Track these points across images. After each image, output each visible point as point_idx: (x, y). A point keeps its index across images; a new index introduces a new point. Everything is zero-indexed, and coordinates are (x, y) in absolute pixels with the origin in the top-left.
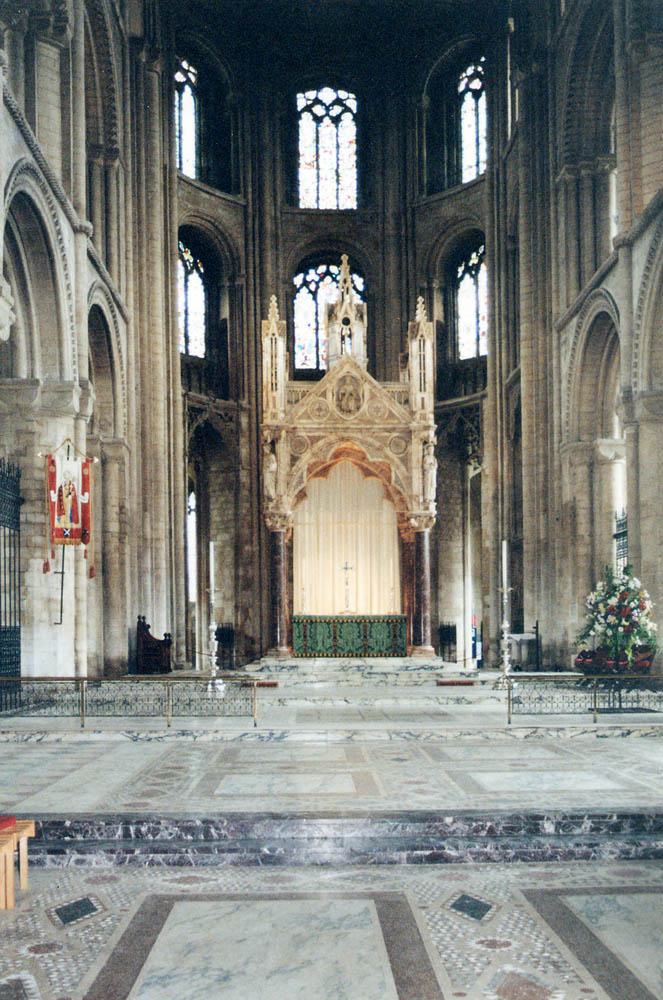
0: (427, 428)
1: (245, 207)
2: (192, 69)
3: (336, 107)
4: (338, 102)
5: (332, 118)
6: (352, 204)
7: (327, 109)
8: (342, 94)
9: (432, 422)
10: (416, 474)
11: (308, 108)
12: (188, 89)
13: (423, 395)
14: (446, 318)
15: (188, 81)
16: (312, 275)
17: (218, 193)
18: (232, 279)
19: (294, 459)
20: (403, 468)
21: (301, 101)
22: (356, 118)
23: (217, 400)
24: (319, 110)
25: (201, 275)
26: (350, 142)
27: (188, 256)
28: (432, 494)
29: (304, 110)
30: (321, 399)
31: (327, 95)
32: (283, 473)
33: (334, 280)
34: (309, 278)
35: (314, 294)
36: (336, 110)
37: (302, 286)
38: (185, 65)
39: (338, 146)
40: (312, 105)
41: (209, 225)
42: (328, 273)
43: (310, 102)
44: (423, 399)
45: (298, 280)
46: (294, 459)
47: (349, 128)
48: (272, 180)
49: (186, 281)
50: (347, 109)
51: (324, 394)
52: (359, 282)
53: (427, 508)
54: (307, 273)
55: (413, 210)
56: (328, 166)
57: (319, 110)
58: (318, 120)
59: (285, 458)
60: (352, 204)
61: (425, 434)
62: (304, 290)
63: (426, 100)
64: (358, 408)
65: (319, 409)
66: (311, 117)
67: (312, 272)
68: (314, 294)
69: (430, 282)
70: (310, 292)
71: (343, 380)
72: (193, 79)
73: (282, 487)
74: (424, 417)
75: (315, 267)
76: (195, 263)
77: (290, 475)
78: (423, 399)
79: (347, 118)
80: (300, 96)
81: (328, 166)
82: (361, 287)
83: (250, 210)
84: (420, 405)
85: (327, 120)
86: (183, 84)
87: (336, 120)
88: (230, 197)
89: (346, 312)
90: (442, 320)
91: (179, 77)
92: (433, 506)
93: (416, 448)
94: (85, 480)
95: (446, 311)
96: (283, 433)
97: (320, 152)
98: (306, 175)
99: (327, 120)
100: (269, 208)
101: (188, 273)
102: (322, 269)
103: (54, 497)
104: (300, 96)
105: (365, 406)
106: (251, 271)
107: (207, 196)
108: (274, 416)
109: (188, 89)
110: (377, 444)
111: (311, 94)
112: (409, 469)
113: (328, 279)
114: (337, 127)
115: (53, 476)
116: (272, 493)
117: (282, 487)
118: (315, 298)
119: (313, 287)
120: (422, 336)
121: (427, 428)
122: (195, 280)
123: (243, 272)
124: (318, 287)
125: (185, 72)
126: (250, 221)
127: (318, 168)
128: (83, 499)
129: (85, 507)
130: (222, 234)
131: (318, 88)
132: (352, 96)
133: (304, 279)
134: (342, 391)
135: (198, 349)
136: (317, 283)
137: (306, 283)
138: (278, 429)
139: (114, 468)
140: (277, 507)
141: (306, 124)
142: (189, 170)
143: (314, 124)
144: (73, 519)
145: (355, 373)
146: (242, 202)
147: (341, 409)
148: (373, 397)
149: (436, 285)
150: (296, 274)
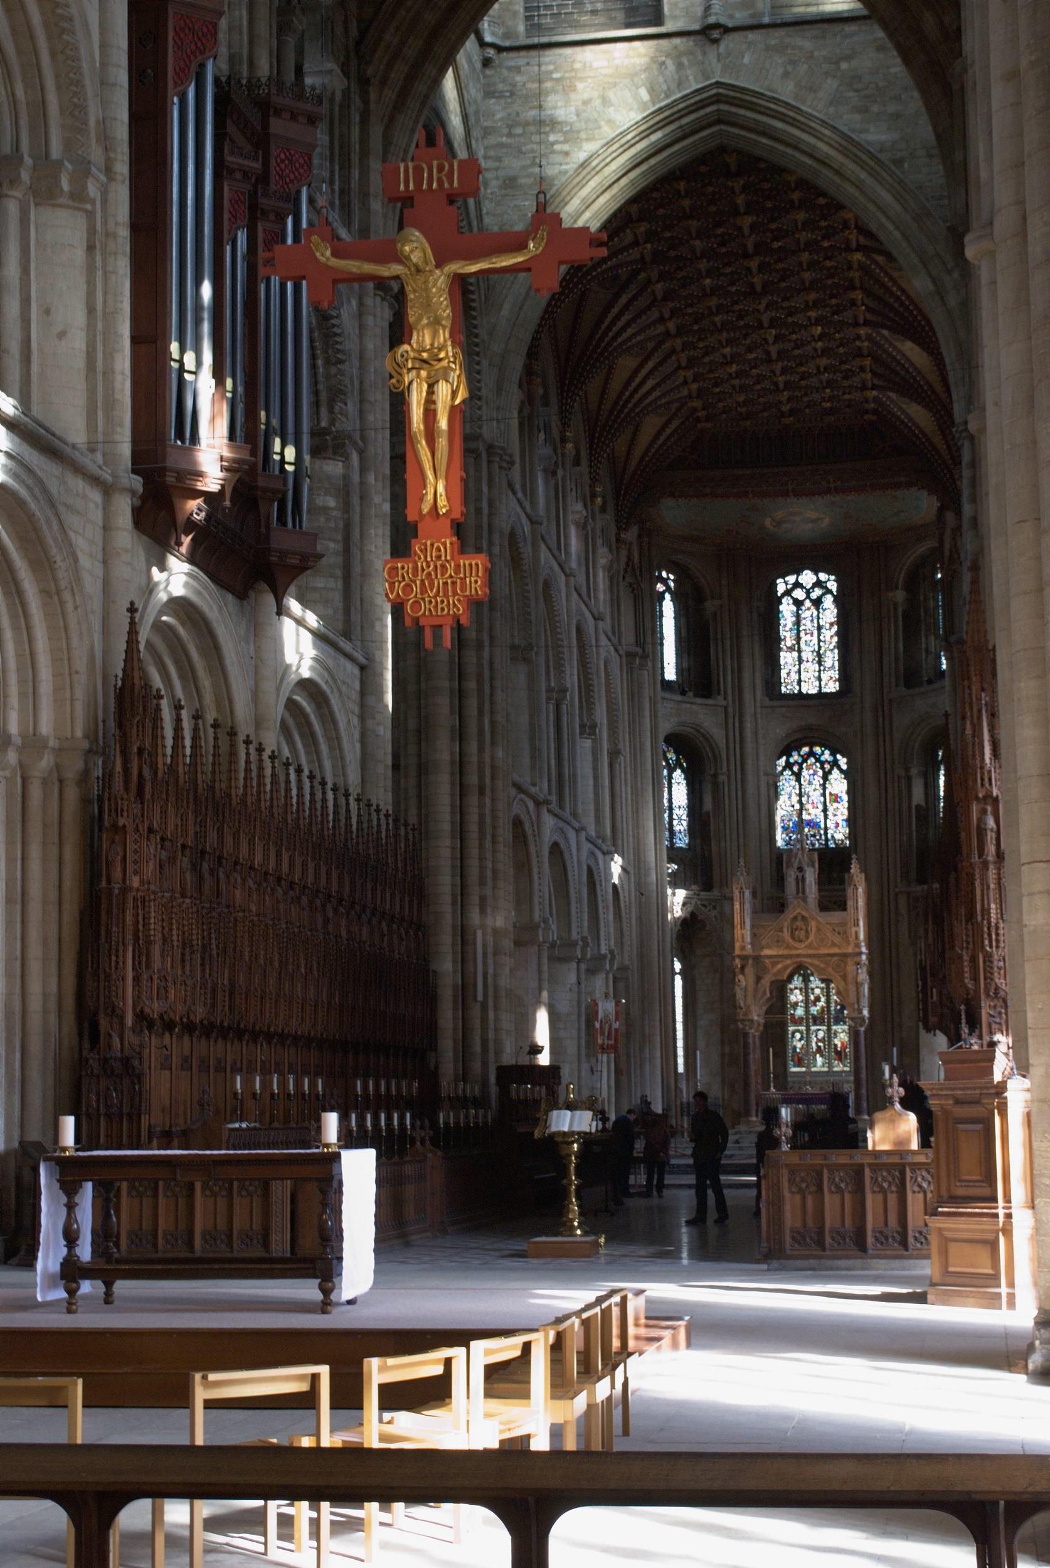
1: (726, 708)
2: (672, 577)
3: (816, 589)
4: (818, 584)
5: (811, 600)
6: (832, 687)
7: (808, 593)
8: (823, 576)
9: (864, 950)
11: (788, 593)
12: (667, 596)
14: (927, 803)
15: (668, 589)
16: (796, 757)
17: (699, 700)
18: (715, 776)
19: (758, 979)
20: (843, 983)
21: (781, 588)
22: (837, 600)
23: (703, 893)
24: (799, 594)
25: (683, 771)
26: (832, 624)
27: (671, 756)
28: (865, 1001)
29: (783, 595)
31: (807, 578)
32: (751, 989)
33: (818, 760)
34: (792, 760)
35: (798, 776)
36: (814, 596)
37: (784, 769)
38: (664, 574)
39: (819, 628)
40: (792, 589)
41: (689, 730)
42: (812, 754)
43: (789, 587)
45: (782, 761)
46: (758, 979)
47: (830, 611)
48: (752, 678)
49: (670, 778)
50: (829, 591)
51: (781, 930)
52: (843, 762)
53: (860, 1011)
54: (789, 756)
55: (891, 701)
56: (810, 650)
57: (799, 594)
58: (798, 603)
59: (751, 978)
60: (832, 687)
62: (787, 772)
63: (900, 596)
64: (807, 938)
65: (778, 941)
66: (791, 601)
67: (795, 754)
68: (798, 776)
69: (907, 770)
70: (793, 773)
71: (795, 919)
72: (672, 584)
73: (750, 1000)
74: (858, 946)
75: (798, 749)
76: (678, 759)
77: (756, 990)
79: (828, 601)
80: (779, 581)
81: (810, 650)
82: (844, 767)
83: (730, 710)
85: (808, 603)
86: (664, 593)
87: (817, 603)
88: (710, 701)
90: (923, 803)
91: (660, 587)
92: (866, 1012)
93: (850, 968)
94: (617, 1013)
95: (926, 794)
96: (750, 961)
97: (802, 634)
98: (787, 659)
99: (808, 603)
100: (749, 708)
101: (671, 771)
102: (806, 749)
103: (597, 1025)
104: (779, 581)
105: (812, 937)
106: (732, 767)
107: (688, 706)
108: (743, 948)
109: (667, 596)
110: (822, 965)
111: (791, 579)
112: (846, 984)
113: (812, 760)
114: (818, 609)
115: (597, 1013)
116: (742, 1004)
117: (750, 1000)
118: (798, 780)
119: (796, 769)
121: (861, 953)
122: (678, 775)
123: (725, 769)
124: (801, 769)
125: (665, 582)
127: (799, 651)
128: (616, 1025)
129: (616, 1030)
130: (703, 736)
131: (798, 572)
132: (833, 578)
133: (787, 761)
135: (682, 841)
136: (800, 765)
137: (789, 766)
138: (744, 958)
140: (746, 1014)
141: (786, 608)
142: (670, 674)
143: (794, 608)
144: (609, 1038)
145: (804, 913)
146: (724, 703)
147: (793, 938)
148: (818, 930)
149: (914, 771)
150: (780, 757)
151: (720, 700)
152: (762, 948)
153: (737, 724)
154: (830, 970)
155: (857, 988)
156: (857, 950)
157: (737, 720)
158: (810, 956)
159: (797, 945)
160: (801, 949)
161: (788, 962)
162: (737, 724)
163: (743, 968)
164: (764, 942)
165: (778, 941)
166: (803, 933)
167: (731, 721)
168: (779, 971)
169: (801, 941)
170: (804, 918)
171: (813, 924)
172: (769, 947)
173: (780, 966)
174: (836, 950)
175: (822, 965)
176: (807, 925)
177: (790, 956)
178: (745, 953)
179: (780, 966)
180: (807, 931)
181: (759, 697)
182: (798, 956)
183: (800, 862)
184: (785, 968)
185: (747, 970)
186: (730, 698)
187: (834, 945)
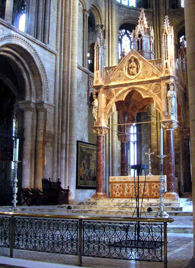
0: (169, 77)
10: (164, 101)
13: (166, 61)
30: (121, 71)
44: (166, 63)
46: (108, 101)
59: (103, 101)
61: (167, 81)
64: (138, 72)
65: (119, 76)
71: (130, 61)
74: (167, 72)
77: (106, 108)
78: (166, 63)
83: (155, 13)
84: (165, 67)
89: (139, 32)
105: (140, 71)
116: (96, 118)
120: (165, 33)
126: (155, 17)
134: (130, 66)
138: (98, 88)
139: (42, 114)
140: (98, 124)
146: (152, 11)
147: (129, 74)
148: (144, 66)
151: (150, 10)
152: (111, 81)
153: (157, 19)
154: (151, 91)
155: (167, 101)
156: (167, 75)
157: (157, 17)
158: (138, 83)
159: (131, 77)
160: (133, 79)
161: (125, 88)
162: (157, 19)
163: (97, 94)
164: (111, 78)
165: (119, 76)
166: (135, 69)
167: (155, 17)
168: (120, 95)
169: (133, 75)
170: (136, 60)
171: (141, 62)
172: (114, 80)
173: (120, 92)
174: (155, 78)
175: (146, 89)
176: (137, 63)
177: (126, 85)
178: (98, 84)
179: (120, 92)
180: (137, 69)
181: (168, 8)
182: (131, 84)
183: (139, 32)
184: (124, 92)
185: (99, 95)
186: (154, 9)
187: (153, 74)
